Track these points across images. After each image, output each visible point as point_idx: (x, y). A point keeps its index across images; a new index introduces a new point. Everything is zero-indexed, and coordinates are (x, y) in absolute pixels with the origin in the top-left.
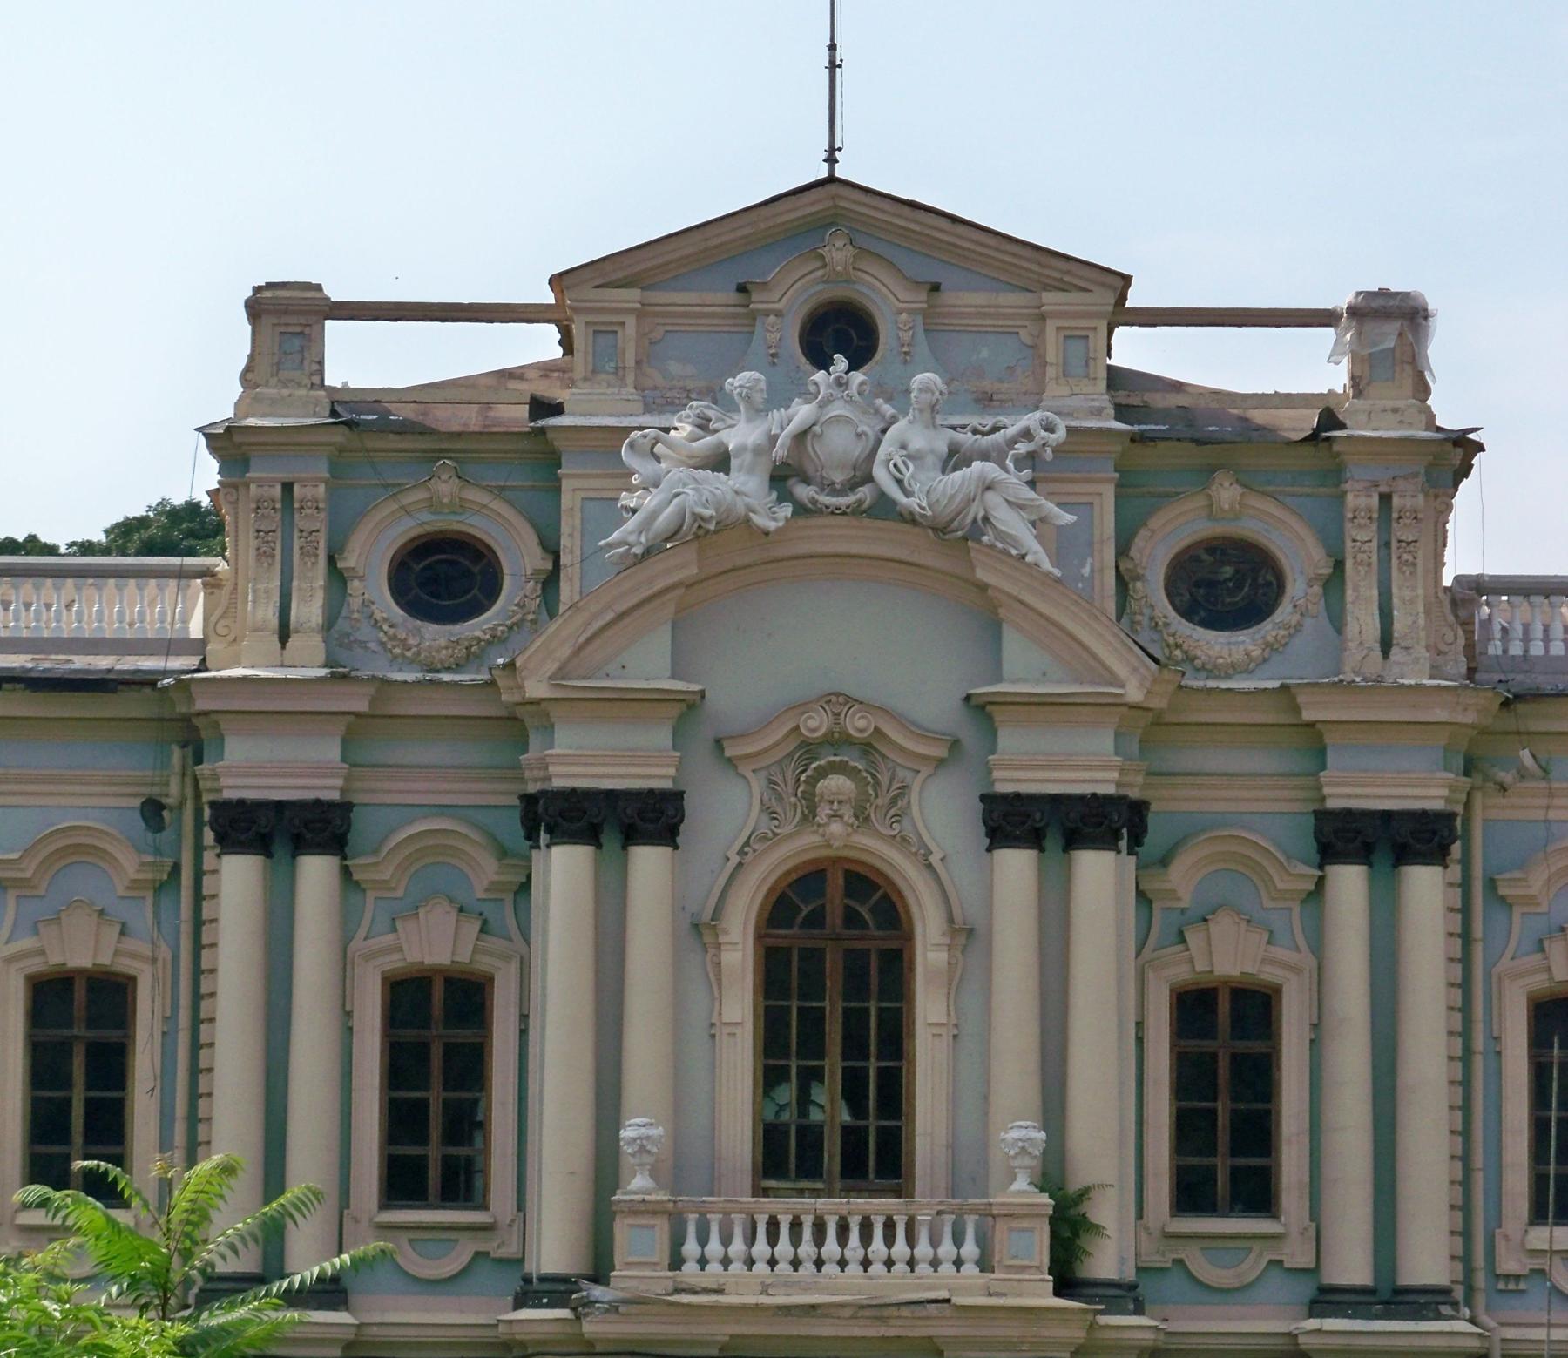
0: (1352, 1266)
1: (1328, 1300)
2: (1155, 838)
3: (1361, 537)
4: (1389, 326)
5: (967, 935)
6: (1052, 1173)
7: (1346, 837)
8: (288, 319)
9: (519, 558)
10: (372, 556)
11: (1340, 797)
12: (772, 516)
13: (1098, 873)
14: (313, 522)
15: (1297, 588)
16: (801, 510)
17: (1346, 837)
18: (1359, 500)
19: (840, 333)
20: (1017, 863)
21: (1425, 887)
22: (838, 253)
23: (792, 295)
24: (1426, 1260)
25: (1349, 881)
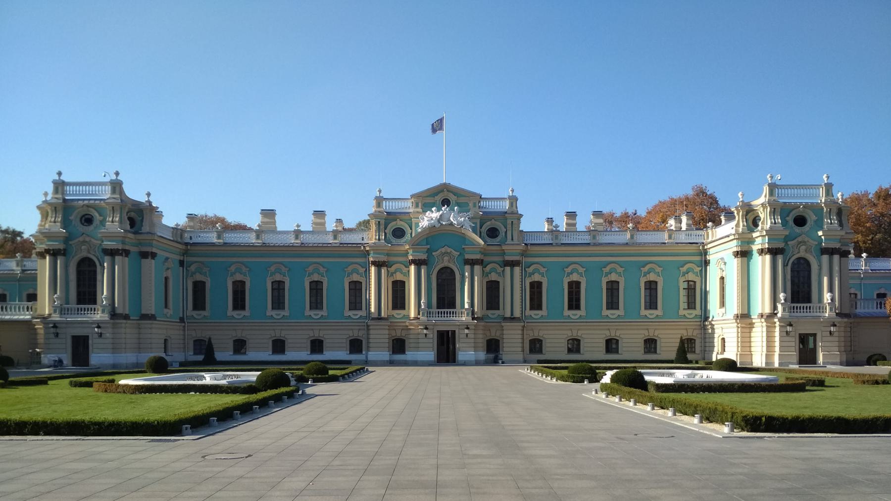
0: (508, 315)
1: (505, 319)
2: (484, 264)
3: (509, 226)
4: (513, 200)
5: (463, 276)
6: (472, 304)
7: (507, 263)
8: (379, 201)
9: (408, 231)
10: (389, 230)
11: (507, 258)
12: (438, 225)
13: (477, 268)
14: (382, 227)
15: (502, 234)
16: (442, 224)
17: (507, 263)
18: (509, 222)
19: (446, 202)
20: (468, 267)
21: (517, 270)
22: (446, 193)
23: (439, 198)
24: (517, 314)
25: (508, 269)
